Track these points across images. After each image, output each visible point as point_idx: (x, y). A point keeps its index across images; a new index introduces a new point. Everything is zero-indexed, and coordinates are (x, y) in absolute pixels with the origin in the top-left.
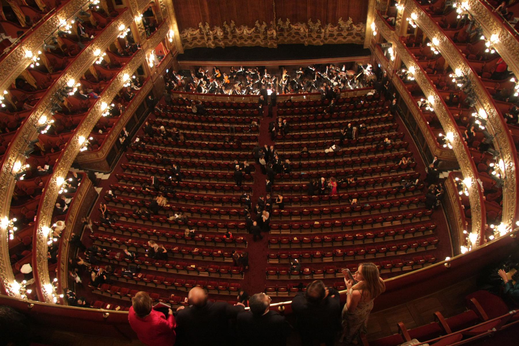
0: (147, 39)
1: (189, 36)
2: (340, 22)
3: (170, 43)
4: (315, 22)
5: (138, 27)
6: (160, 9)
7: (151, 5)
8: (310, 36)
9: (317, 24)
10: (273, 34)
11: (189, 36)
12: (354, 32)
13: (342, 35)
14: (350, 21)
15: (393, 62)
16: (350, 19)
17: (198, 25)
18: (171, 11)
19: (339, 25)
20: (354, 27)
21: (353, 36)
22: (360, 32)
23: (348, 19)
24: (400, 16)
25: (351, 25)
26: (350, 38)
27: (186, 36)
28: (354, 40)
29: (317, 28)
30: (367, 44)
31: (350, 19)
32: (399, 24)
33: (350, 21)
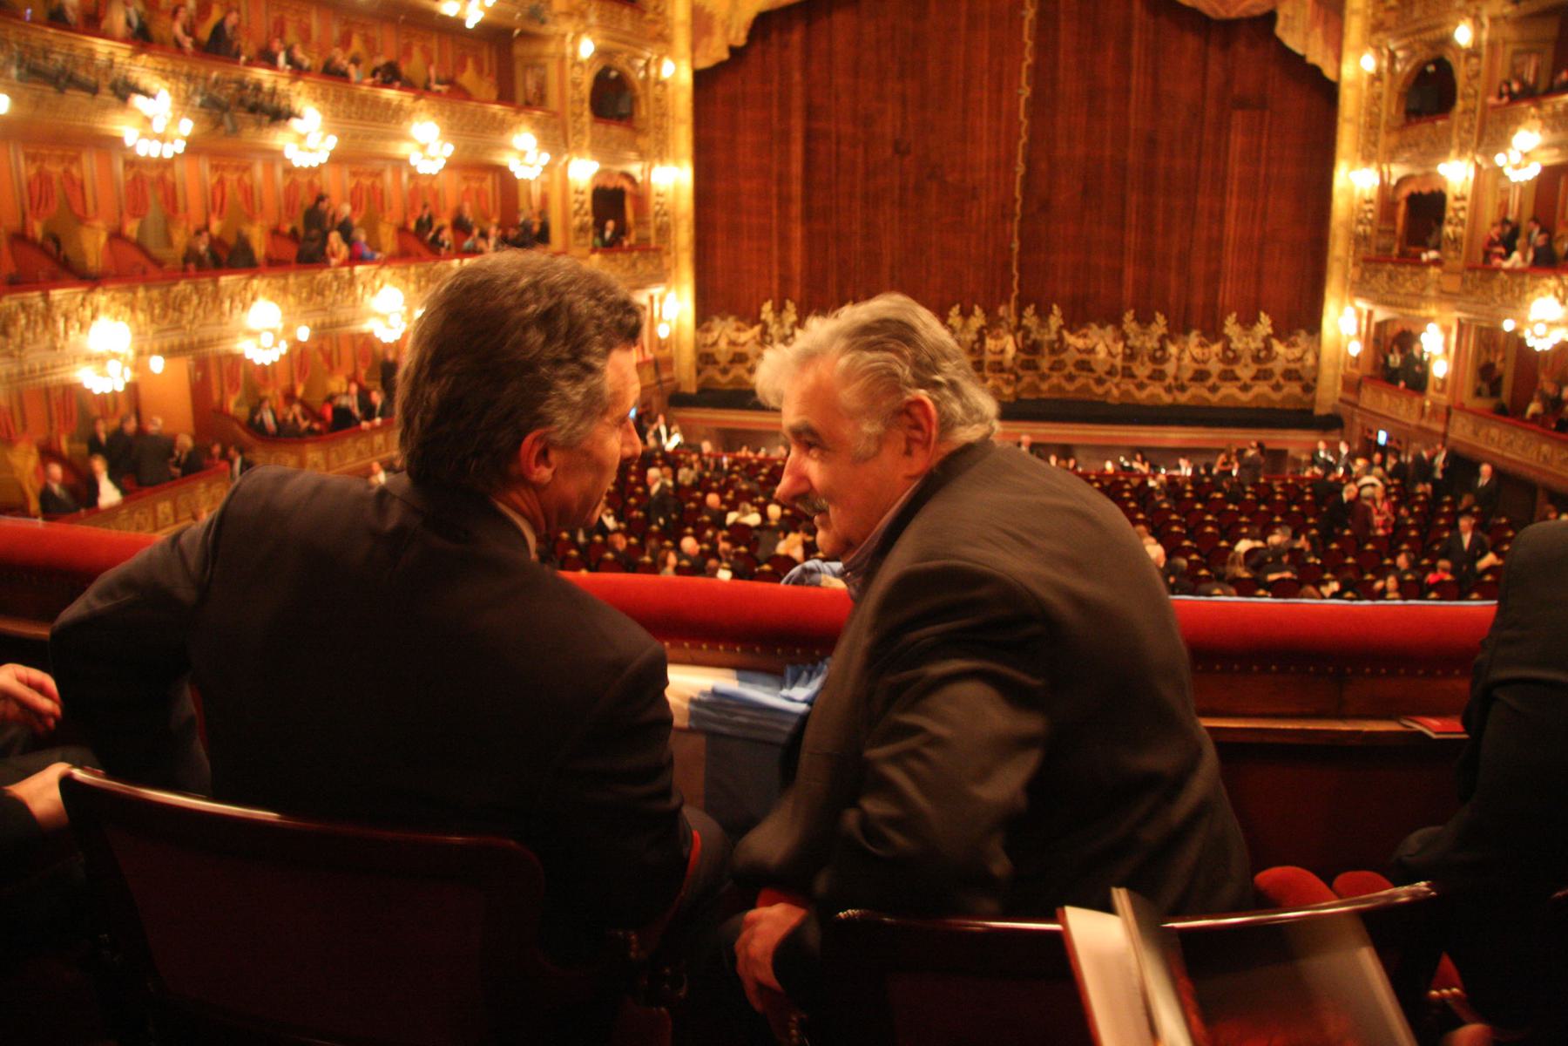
0: (594, 250)
1: (723, 345)
2: (1231, 327)
3: (660, 341)
4: (1144, 320)
5: (573, 197)
6: (652, 214)
7: (626, 185)
8: (1128, 373)
9: (1154, 327)
10: (1002, 351)
11: (723, 345)
12: (1278, 366)
13: (1237, 379)
14: (1264, 326)
15: (1444, 381)
16: (1265, 319)
17: (759, 313)
18: (684, 236)
19: (1228, 340)
20: (1279, 348)
21: (1273, 381)
22: (1297, 366)
23: (1256, 320)
24: (1458, 205)
25: (1266, 340)
26: (1262, 388)
27: (715, 344)
28: (1276, 396)
29: (1152, 344)
30: (1328, 394)
31: (1265, 319)
32: (1459, 229)
33: (1264, 326)
